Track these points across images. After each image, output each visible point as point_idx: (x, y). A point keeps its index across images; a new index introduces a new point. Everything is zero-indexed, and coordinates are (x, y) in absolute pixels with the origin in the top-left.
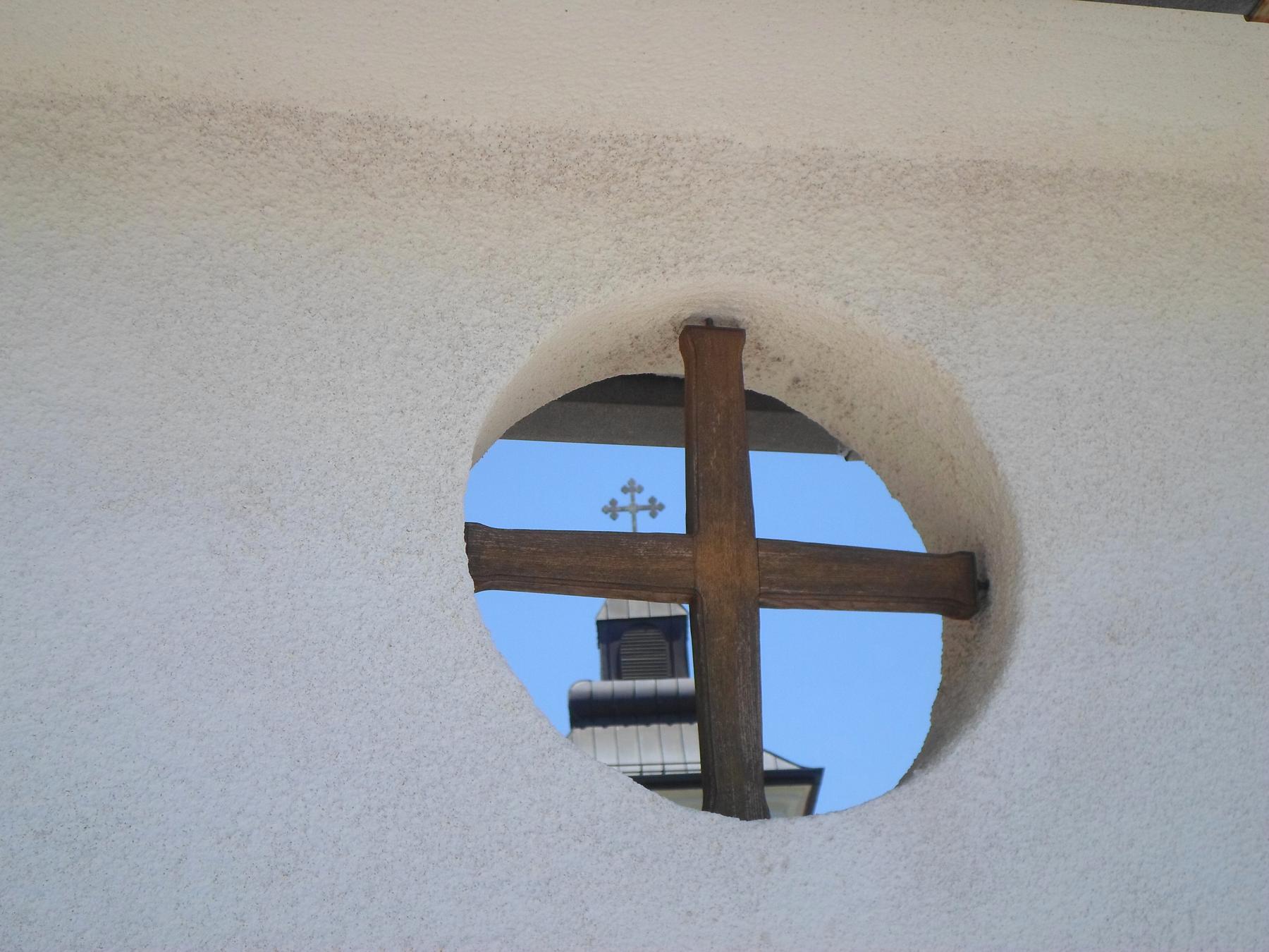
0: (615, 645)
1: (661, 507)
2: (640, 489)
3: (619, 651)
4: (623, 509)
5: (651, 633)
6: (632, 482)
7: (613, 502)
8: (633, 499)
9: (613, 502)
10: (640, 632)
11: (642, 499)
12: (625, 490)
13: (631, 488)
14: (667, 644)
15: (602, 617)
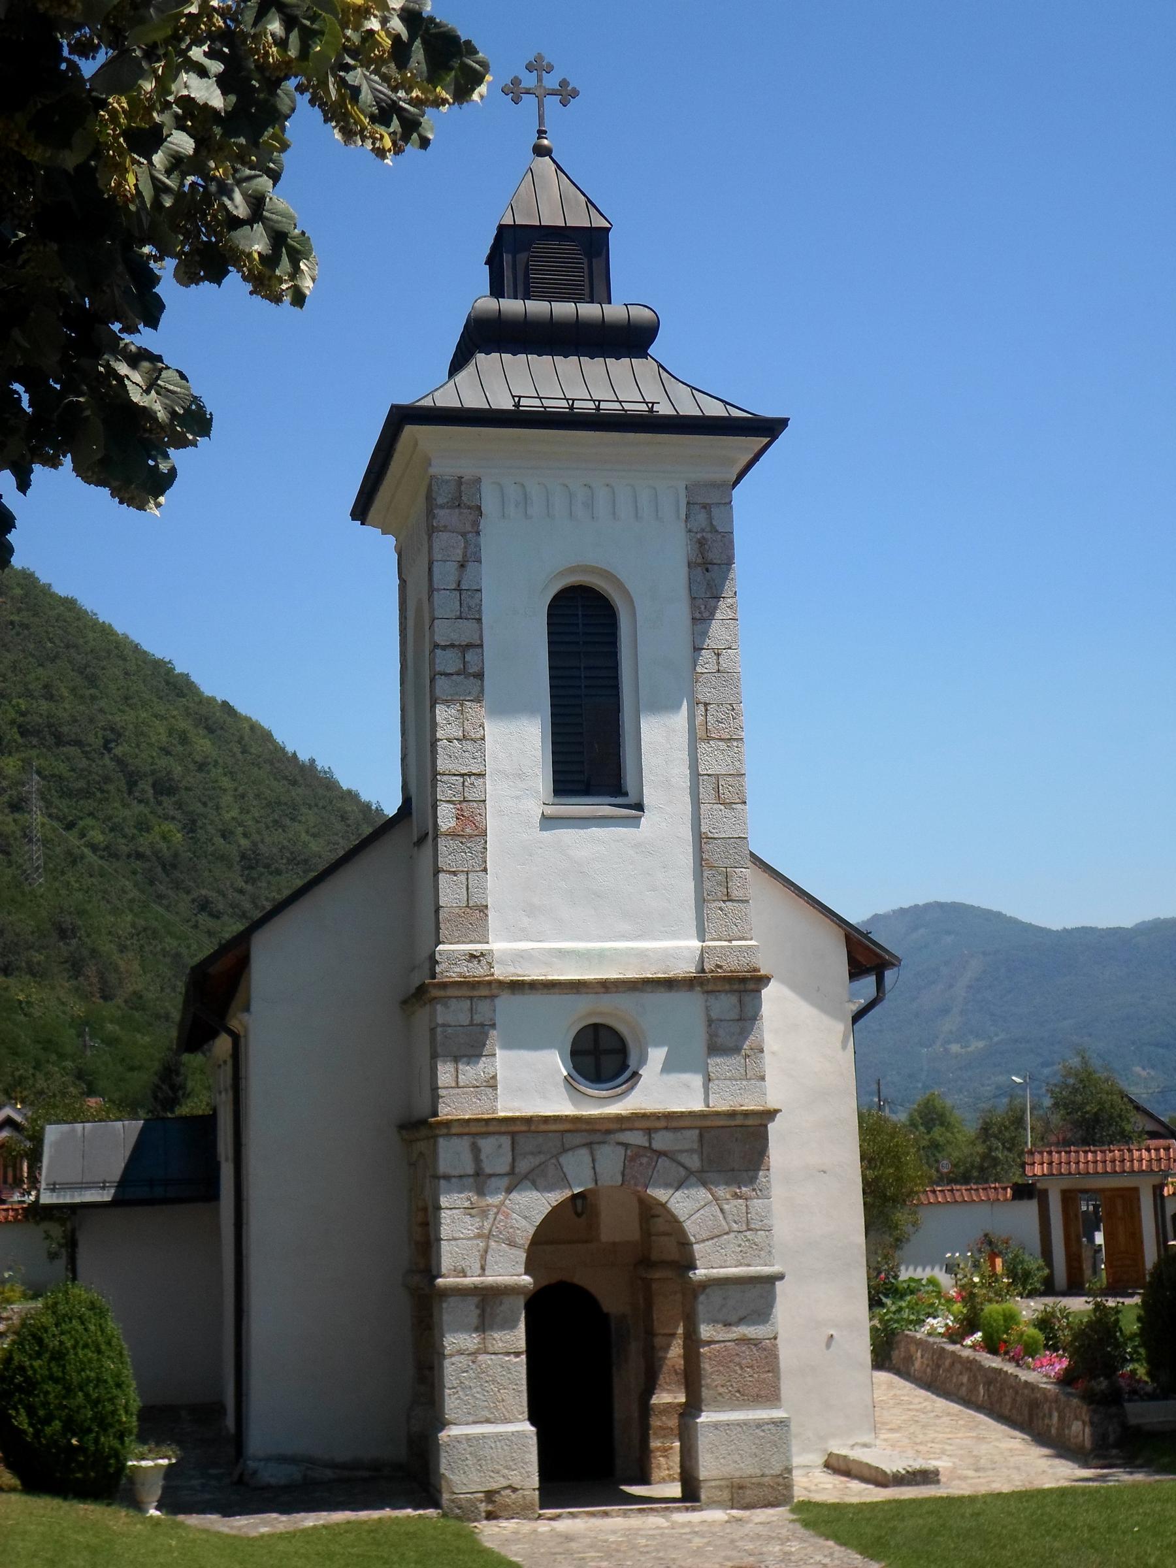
0: (522, 257)
1: (574, 94)
2: (549, 69)
3: (527, 265)
4: (528, 92)
5: (567, 246)
6: (539, 58)
7: (516, 81)
8: (540, 80)
9: (516, 81)
10: (554, 244)
11: (551, 81)
12: (530, 68)
13: (537, 66)
14: (585, 261)
15: (508, 221)
